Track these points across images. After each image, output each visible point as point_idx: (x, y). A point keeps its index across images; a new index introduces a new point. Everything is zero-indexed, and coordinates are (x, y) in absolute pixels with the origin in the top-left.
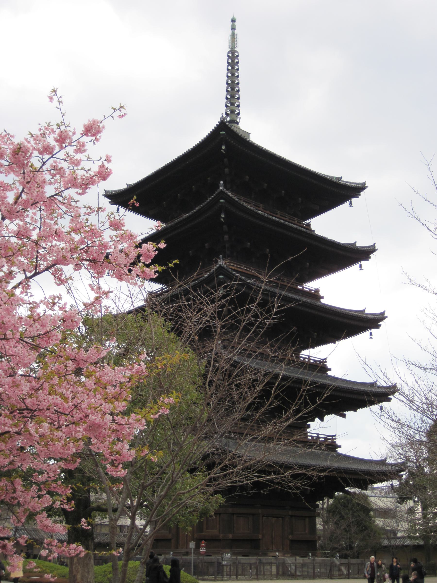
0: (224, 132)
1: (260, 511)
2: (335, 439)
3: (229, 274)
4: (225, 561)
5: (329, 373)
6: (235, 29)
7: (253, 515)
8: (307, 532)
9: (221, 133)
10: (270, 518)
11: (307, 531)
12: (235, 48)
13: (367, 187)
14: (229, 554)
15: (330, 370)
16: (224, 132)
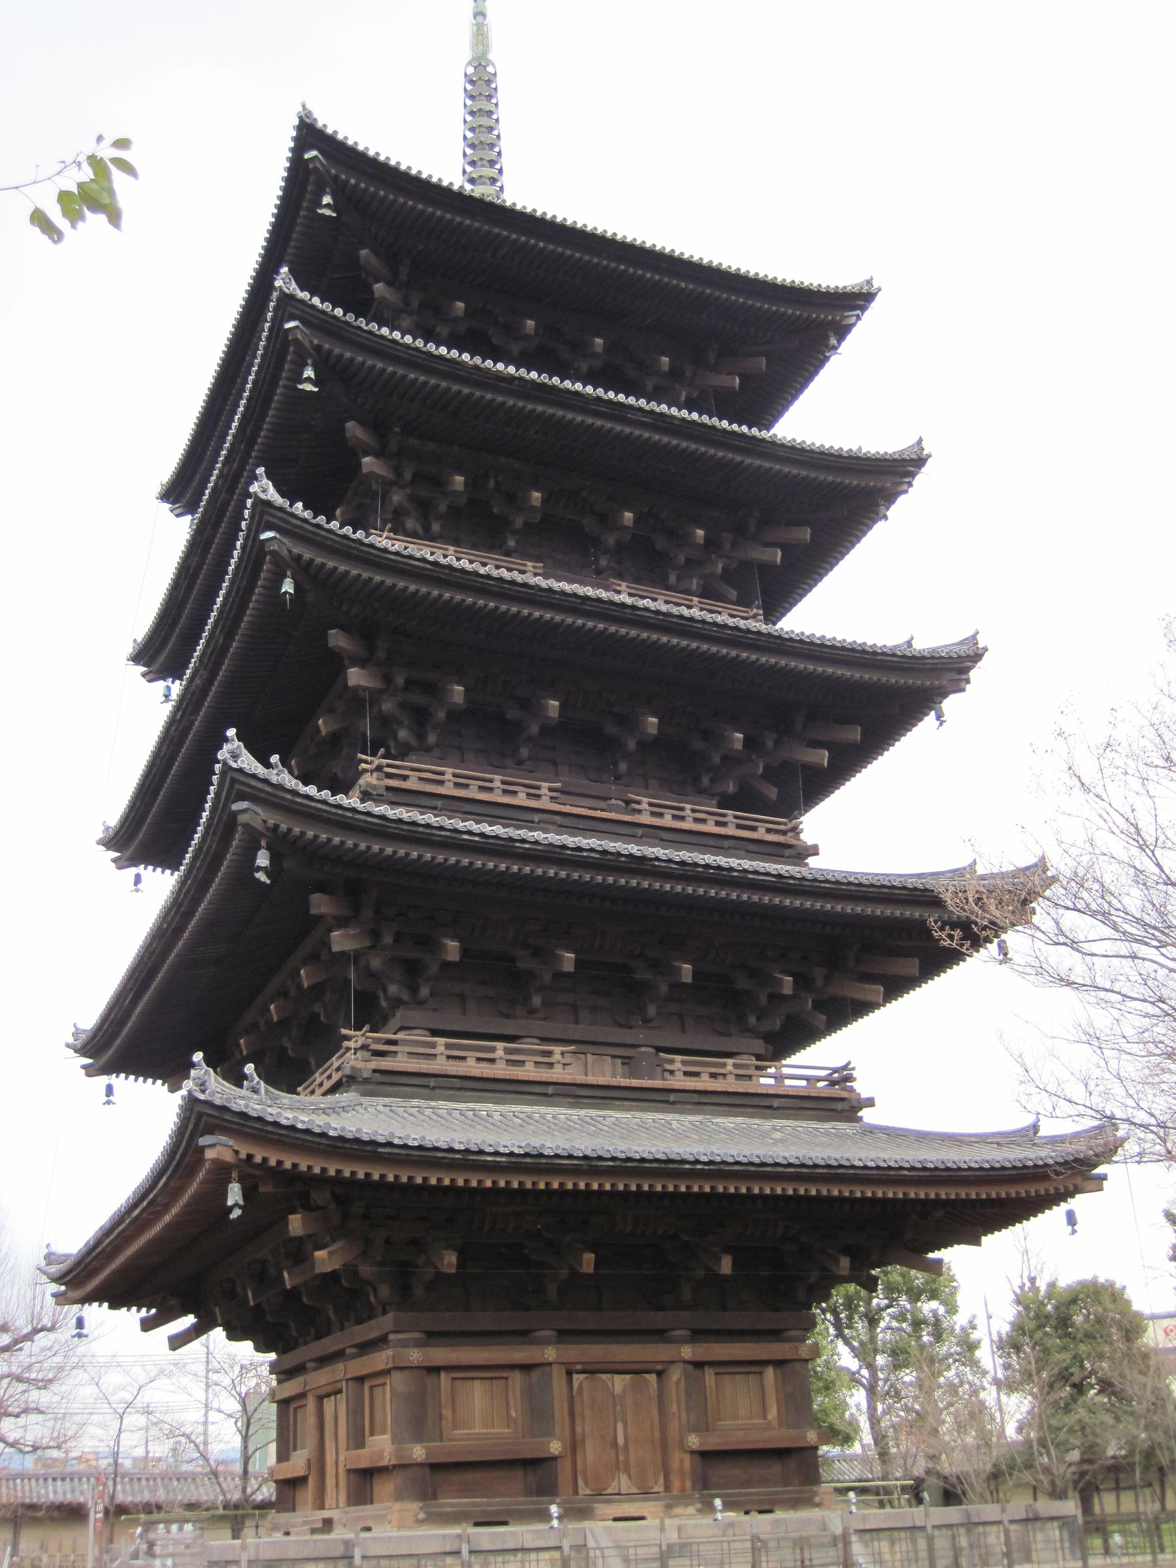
0: (314, 153)
1: (550, 1353)
2: (850, 1078)
3: (299, 523)
4: (162, 1556)
5: (812, 862)
6: (484, 15)
7: (526, 1368)
8: (770, 1417)
9: (306, 156)
10: (604, 1376)
11: (773, 1413)
12: (485, 53)
13: (880, 290)
14: (188, 1527)
15: (814, 851)
16: (314, 153)
